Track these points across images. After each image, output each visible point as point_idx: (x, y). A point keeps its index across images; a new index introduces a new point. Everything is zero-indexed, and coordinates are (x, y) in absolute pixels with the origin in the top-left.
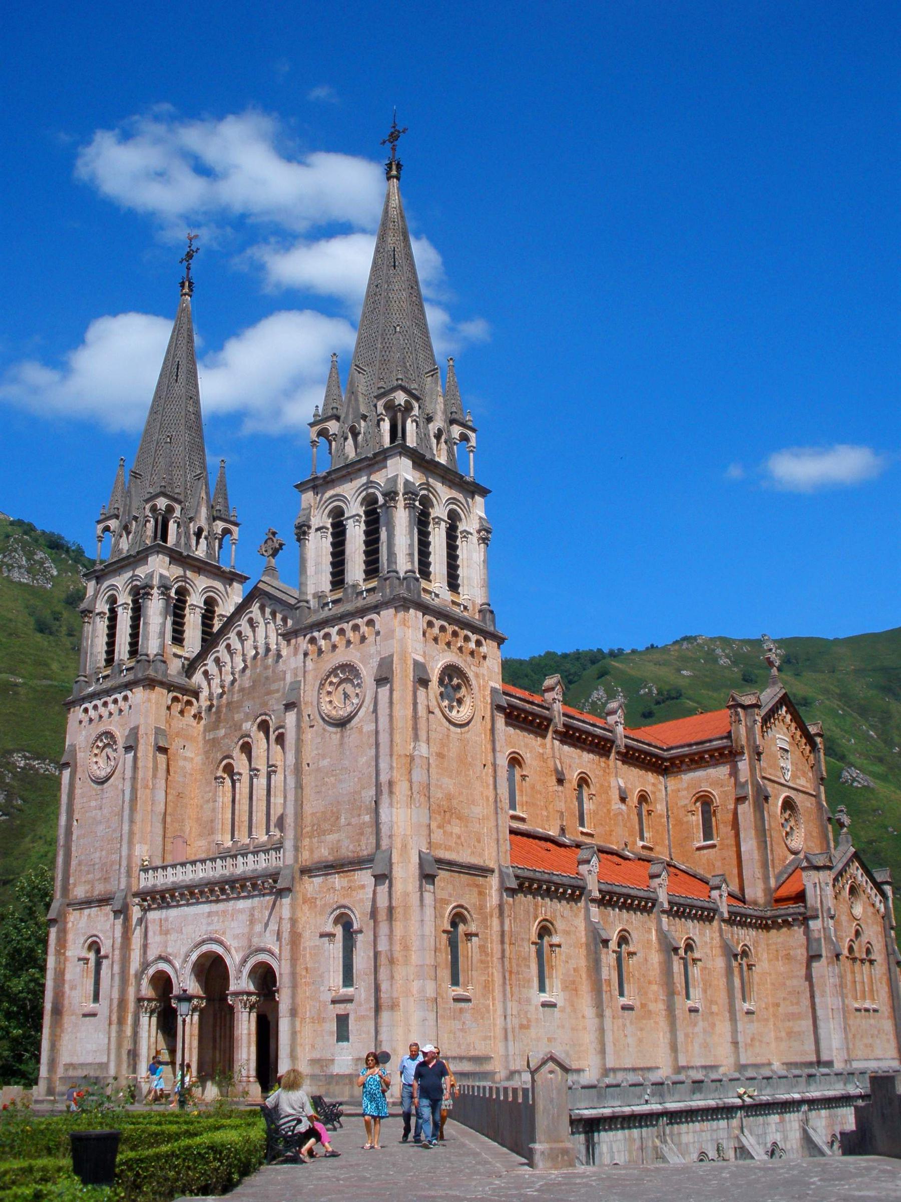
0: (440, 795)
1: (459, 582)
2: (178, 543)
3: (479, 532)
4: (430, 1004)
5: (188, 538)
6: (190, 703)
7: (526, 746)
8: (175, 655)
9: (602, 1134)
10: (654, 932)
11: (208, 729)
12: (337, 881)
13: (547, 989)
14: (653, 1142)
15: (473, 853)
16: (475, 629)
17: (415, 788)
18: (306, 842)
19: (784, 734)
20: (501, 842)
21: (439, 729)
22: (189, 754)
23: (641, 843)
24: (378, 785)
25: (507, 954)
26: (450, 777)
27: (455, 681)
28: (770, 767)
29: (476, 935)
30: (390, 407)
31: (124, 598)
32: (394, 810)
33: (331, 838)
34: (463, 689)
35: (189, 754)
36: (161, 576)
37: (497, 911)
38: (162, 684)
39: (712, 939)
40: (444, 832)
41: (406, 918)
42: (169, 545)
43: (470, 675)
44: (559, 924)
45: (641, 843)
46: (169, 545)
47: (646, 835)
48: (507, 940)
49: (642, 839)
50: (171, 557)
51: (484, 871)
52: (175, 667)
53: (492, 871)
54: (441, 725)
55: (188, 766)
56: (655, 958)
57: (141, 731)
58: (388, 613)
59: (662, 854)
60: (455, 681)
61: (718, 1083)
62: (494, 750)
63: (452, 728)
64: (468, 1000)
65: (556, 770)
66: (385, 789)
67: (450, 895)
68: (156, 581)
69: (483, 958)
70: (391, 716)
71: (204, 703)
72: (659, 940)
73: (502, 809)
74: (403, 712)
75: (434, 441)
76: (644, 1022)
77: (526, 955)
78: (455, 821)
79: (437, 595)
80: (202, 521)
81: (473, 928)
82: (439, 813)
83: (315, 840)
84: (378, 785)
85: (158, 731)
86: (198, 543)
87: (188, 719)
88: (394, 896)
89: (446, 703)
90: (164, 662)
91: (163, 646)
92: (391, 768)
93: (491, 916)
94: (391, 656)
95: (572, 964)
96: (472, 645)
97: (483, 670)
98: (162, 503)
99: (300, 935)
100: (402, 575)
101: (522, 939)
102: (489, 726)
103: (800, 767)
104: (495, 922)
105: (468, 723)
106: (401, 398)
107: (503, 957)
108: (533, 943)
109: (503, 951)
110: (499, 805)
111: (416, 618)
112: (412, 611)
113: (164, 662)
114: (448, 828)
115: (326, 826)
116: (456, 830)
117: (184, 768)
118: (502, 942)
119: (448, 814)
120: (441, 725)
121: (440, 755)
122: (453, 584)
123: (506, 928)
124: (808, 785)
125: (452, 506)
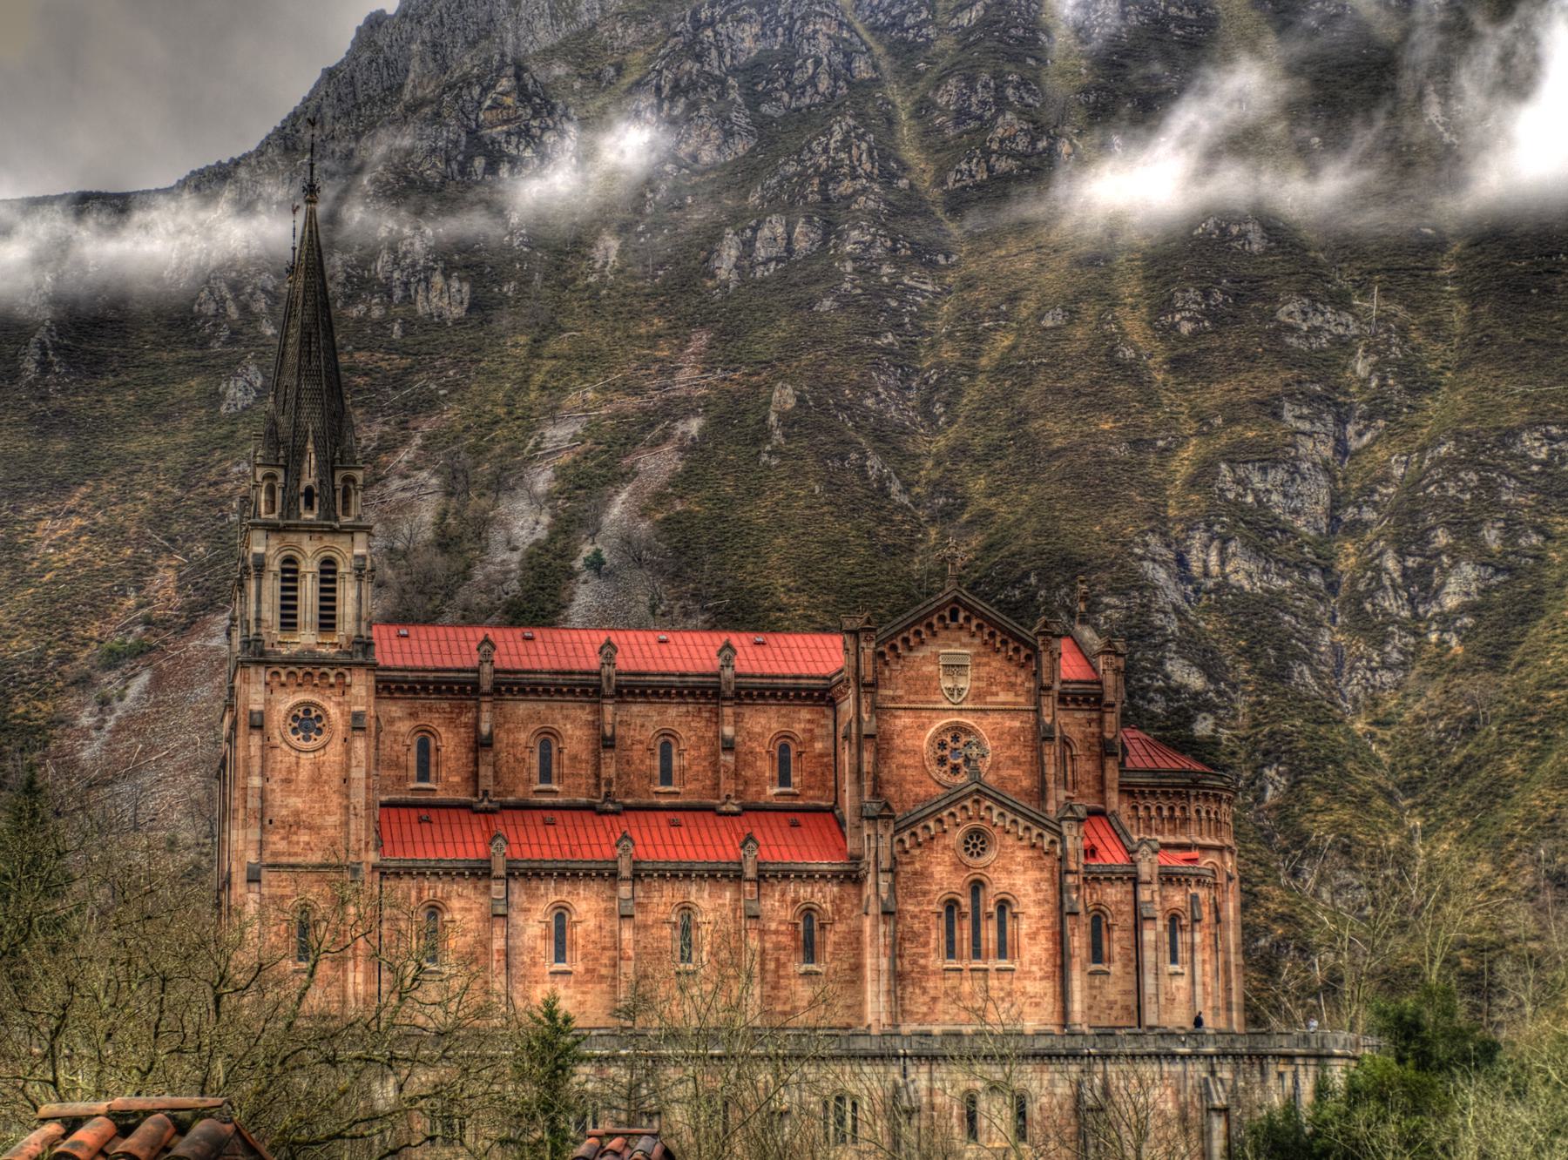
0: (284, 812)
7: (566, 717)
19: (964, 645)
23: (777, 790)
27: (313, 715)
28: (916, 693)
40: (290, 843)
47: (795, 779)
49: (784, 780)
59: (820, 798)
60: (313, 715)
63: (303, 756)
65: (604, 738)
75: (302, 500)
96: (332, 680)
97: (347, 698)
103: (1002, 678)
114: (295, 838)
116: (306, 838)
124: (1022, 699)
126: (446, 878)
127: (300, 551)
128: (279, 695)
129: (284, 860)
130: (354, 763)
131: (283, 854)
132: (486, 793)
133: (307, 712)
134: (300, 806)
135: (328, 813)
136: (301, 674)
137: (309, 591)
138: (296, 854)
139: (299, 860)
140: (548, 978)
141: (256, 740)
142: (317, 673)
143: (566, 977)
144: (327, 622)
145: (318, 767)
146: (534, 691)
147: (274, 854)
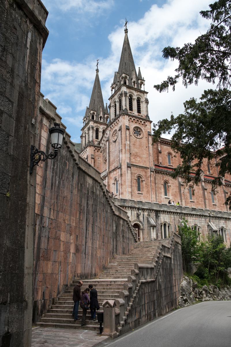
1: (141, 111)
2: (96, 120)
3: (145, 101)
4: (129, 193)
5: (99, 118)
6: (99, 150)
8: (96, 141)
9: (161, 214)
10: (201, 186)
11: (103, 154)
12: (115, 172)
13: (167, 195)
14: (178, 219)
15: (143, 164)
16: (143, 119)
17: (126, 150)
18: (110, 167)
20: (150, 162)
21: (133, 139)
22: (99, 159)
23: (209, 173)
24: (119, 151)
25: (152, 185)
26: (137, 149)
27: (139, 130)
29: (144, 181)
30: (122, 78)
31: (87, 132)
32: (122, 155)
33: (114, 164)
34: (141, 132)
35: (99, 159)
36: (92, 126)
37: (150, 177)
38: (92, 146)
39: (221, 190)
40: (135, 160)
41: (125, 176)
42: (94, 120)
43: (142, 129)
44: (170, 182)
45: (209, 173)
46: (94, 120)
47: (211, 171)
48: (152, 182)
49: (209, 172)
50: (94, 122)
51: (147, 168)
52: (96, 143)
53: (149, 168)
54: (134, 138)
55: (100, 162)
56: (201, 192)
57: (89, 155)
58: (121, 117)
60: (139, 130)
61: (202, 210)
62: (148, 144)
63: (137, 139)
64: (142, 194)
66: (120, 151)
67: (137, 172)
68: (91, 127)
69: (146, 186)
70: (121, 137)
71: (102, 149)
72: (202, 188)
73: (151, 155)
74: (123, 136)
75: (133, 83)
76: (198, 206)
77: (160, 187)
78: (138, 158)
79: (134, 114)
80: (101, 115)
81: (143, 179)
82: (134, 156)
83: (112, 166)
84: (119, 151)
85: (92, 155)
86: (101, 119)
87: (99, 153)
88: (122, 172)
89: (136, 134)
90: (93, 142)
91: (93, 139)
92: (121, 147)
93: (149, 177)
94: (121, 126)
95: (174, 190)
96: (143, 123)
97: (146, 128)
98: (92, 112)
99: (110, 185)
100: (124, 109)
101: (159, 184)
102: (148, 139)
104: (150, 179)
105: (142, 138)
106: (124, 75)
107: (151, 185)
108: (162, 185)
109: (151, 184)
110: (150, 154)
111: (127, 118)
112: (126, 116)
113: (93, 142)
114: (136, 159)
115: (113, 162)
116: (139, 160)
117: (98, 162)
118: (151, 183)
119: (136, 156)
120: (134, 138)
121: (134, 144)
122: (139, 111)
123: (152, 179)
125: (138, 96)
126: (168, 175)
127: (133, 94)
128: (131, 123)
129: (134, 164)
130: (149, 143)
131: (134, 162)
132: (161, 163)
133: (137, 129)
134: (137, 151)
135: (143, 154)
136: (136, 120)
137: (135, 103)
138: (137, 163)
139: (138, 165)
140: (190, 202)
141: (128, 132)
142: (140, 121)
143: (193, 203)
144: (139, 111)
145: (141, 143)
146: (167, 144)
147: (132, 162)
